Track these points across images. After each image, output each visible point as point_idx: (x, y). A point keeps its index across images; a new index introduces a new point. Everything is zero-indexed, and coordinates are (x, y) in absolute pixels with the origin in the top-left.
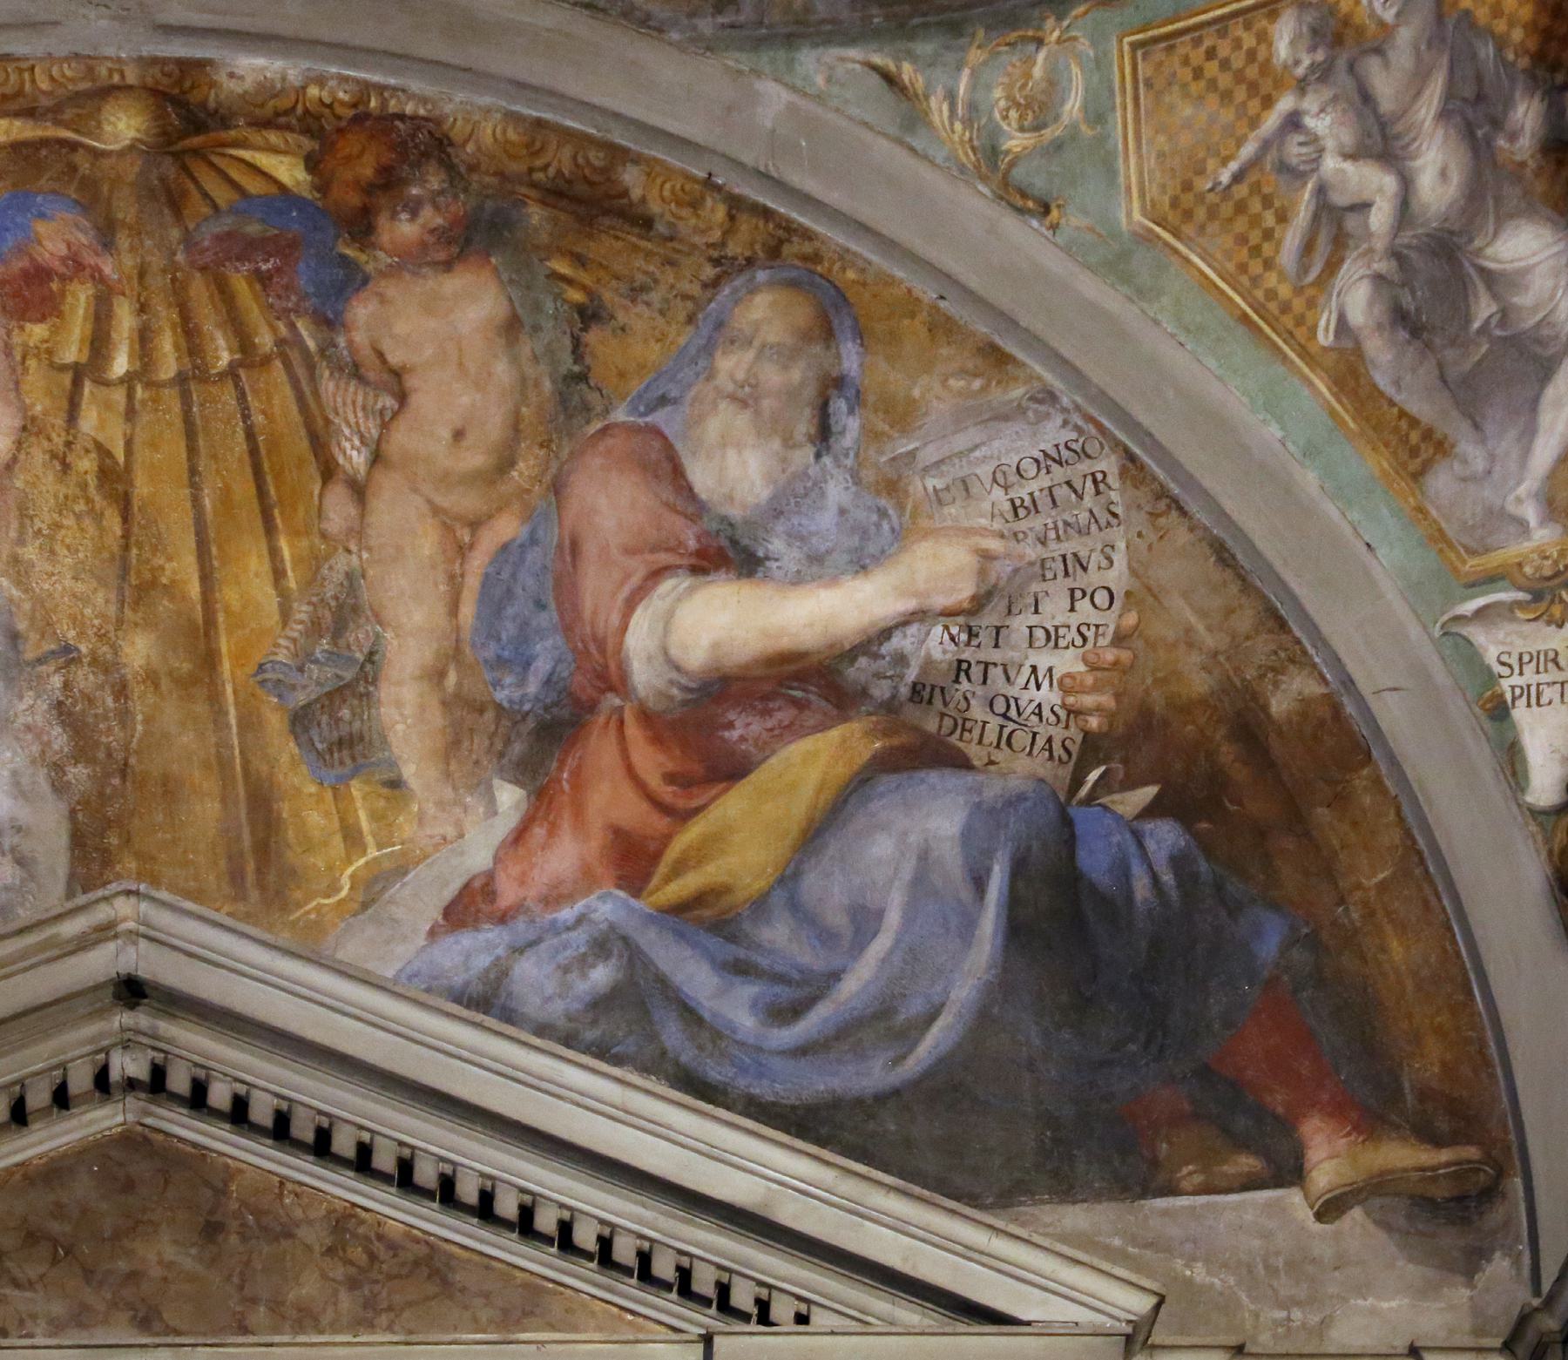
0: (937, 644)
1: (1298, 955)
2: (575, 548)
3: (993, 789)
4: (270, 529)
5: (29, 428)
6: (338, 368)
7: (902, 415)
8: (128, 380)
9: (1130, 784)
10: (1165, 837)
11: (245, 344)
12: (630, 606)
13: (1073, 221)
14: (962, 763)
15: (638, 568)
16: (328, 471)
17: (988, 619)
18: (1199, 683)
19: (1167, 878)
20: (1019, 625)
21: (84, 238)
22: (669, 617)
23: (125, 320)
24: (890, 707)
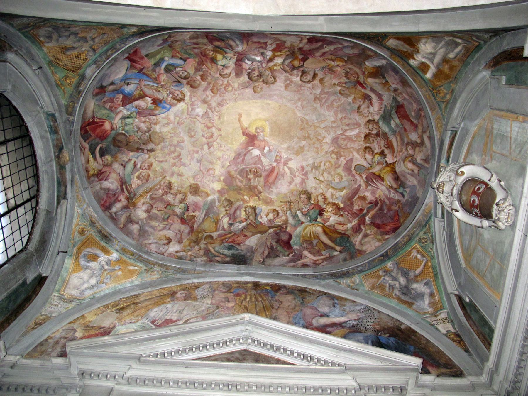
0: (355, 323)
1: (416, 350)
2: (305, 314)
3: (366, 335)
4: (265, 311)
5: (236, 304)
6: (274, 301)
7: (344, 305)
8: (249, 301)
9: (385, 334)
10: (392, 339)
11: (263, 299)
12: (312, 319)
13: (360, 290)
14: (361, 332)
15: (313, 316)
16: (273, 308)
17: (360, 321)
18: (391, 326)
19: (394, 342)
20: (365, 321)
21: (244, 291)
22: (317, 321)
23: (249, 297)
24: (349, 328)
